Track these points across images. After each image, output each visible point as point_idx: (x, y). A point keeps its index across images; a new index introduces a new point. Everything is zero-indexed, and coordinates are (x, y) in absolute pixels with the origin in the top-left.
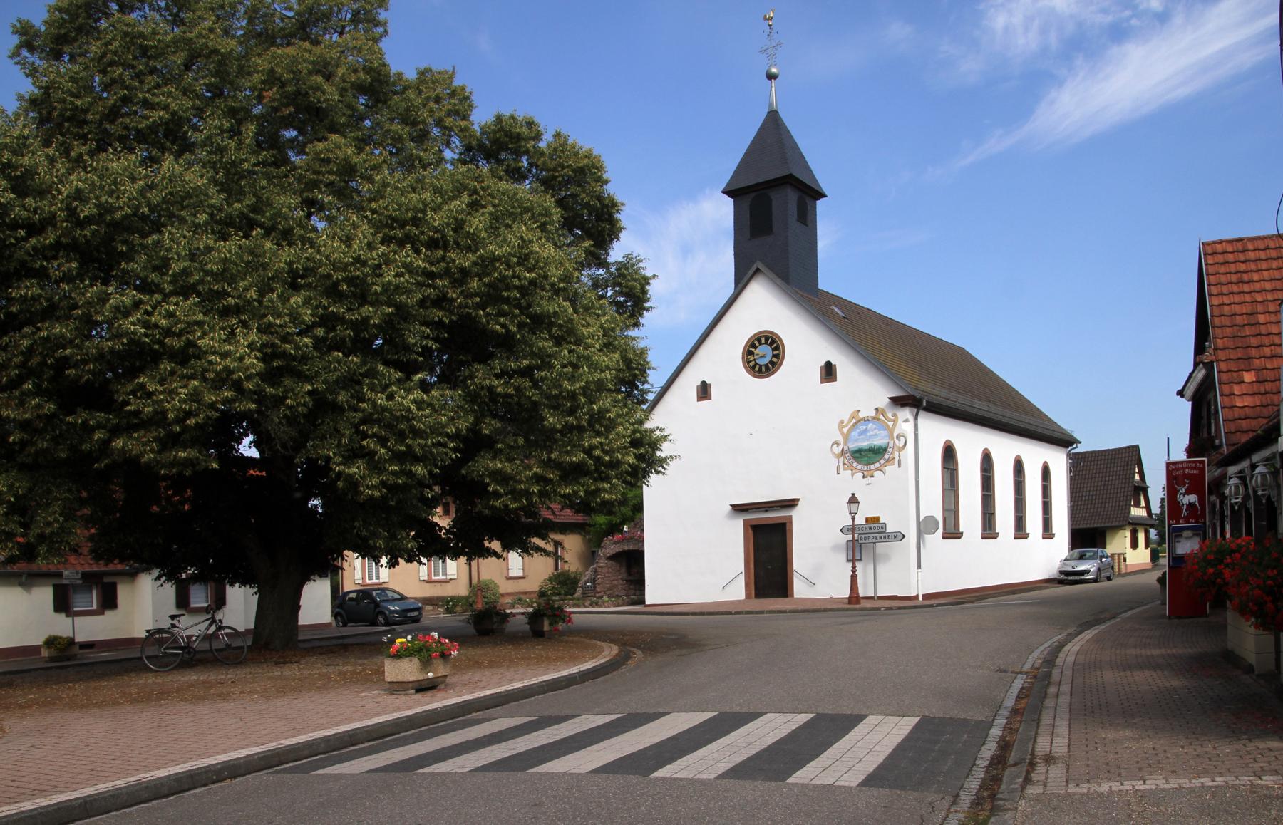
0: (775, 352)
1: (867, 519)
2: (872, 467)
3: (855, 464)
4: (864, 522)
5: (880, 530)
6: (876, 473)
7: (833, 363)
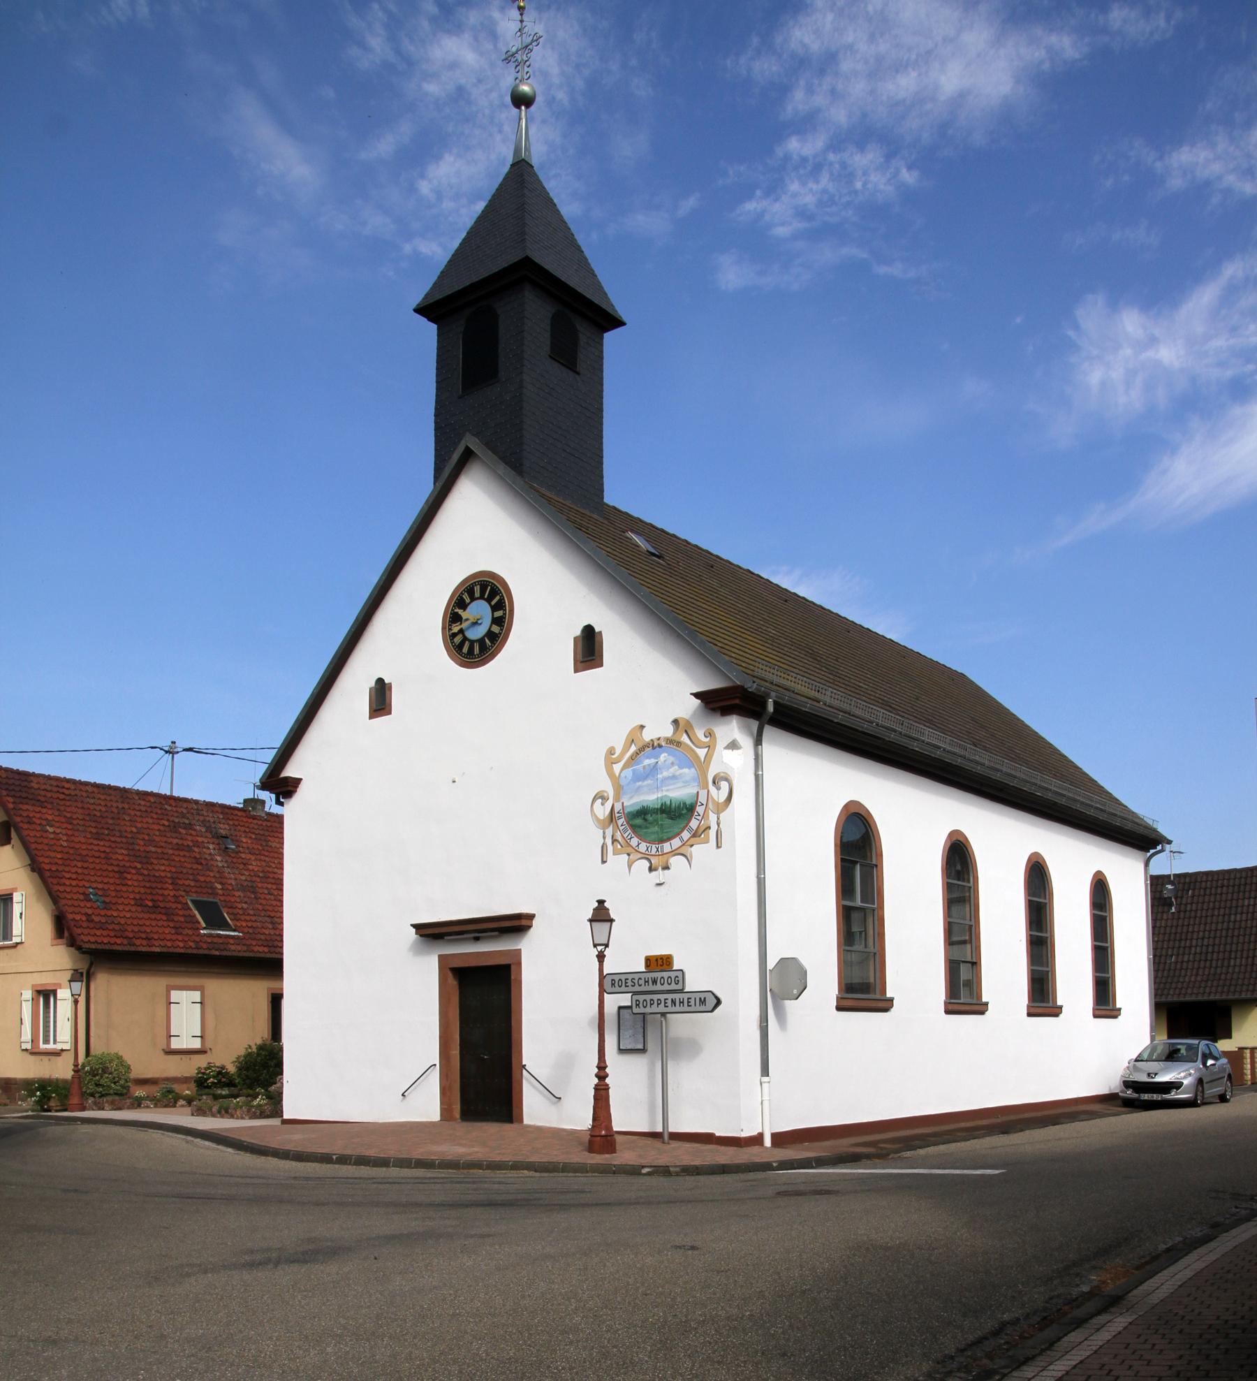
0: (498, 614)
1: (649, 961)
2: (667, 847)
3: (634, 841)
4: (641, 967)
5: (673, 987)
6: (676, 861)
7: (597, 630)
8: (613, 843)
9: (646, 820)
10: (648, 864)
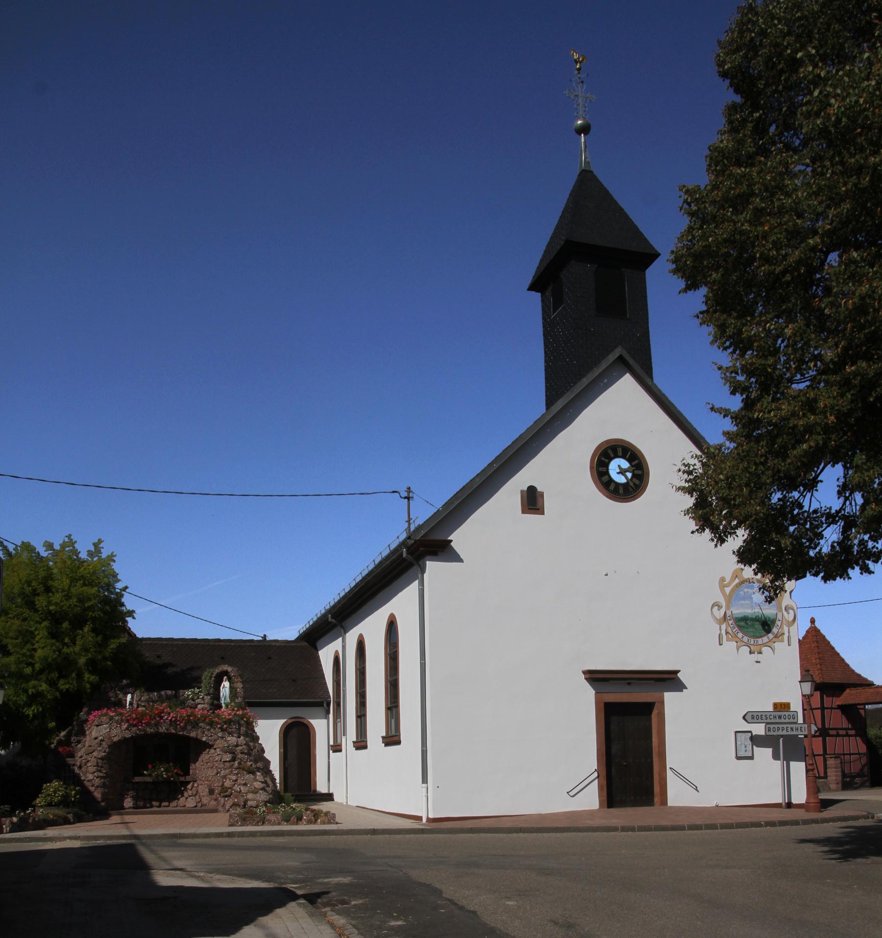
1: (776, 705)
2: (760, 641)
3: (740, 635)
5: (791, 720)
6: (765, 649)
8: (726, 634)
9: (747, 624)
10: (749, 650)
